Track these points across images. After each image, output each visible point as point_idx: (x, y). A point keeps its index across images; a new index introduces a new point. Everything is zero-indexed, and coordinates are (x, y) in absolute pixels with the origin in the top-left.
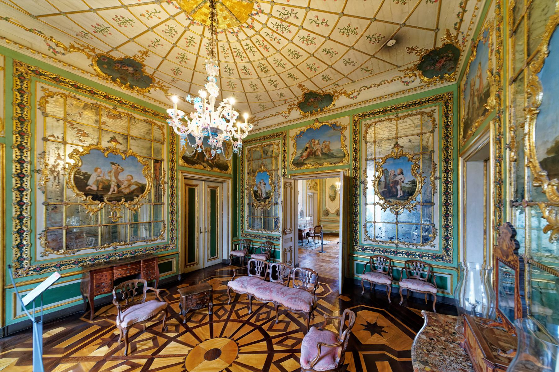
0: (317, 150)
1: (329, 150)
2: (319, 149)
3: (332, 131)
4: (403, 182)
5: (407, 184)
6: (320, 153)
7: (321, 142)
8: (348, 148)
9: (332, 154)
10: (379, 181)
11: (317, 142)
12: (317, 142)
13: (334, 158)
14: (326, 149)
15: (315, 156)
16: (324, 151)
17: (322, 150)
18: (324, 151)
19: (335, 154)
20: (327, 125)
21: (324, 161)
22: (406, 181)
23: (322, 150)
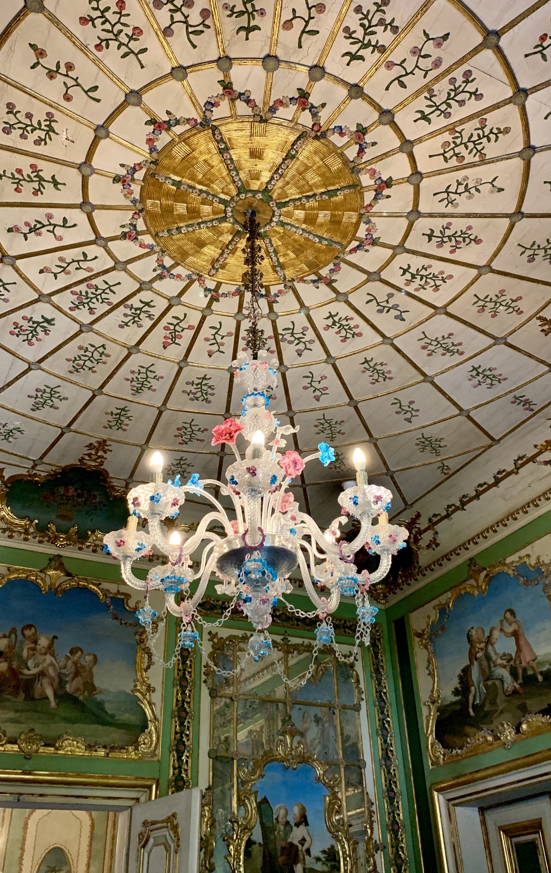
0: (42, 674)
1: (90, 687)
2: (51, 672)
3: (109, 621)
4: (308, 851)
5: (318, 859)
6: (50, 692)
7: (63, 651)
8: (157, 697)
9: (100, 705)
10: (250, 843)
11: (43, 642)
12: (43, 642)
13: (104, 723)
14: (78, 682)
15: (30, 697)
16: (69, 688)
17: (62, 682)
18: (69, 688)
19: (108, 707)
20: (96, 594)
21: (59, 727)
22: (316, 852)
23: (62, 682)
